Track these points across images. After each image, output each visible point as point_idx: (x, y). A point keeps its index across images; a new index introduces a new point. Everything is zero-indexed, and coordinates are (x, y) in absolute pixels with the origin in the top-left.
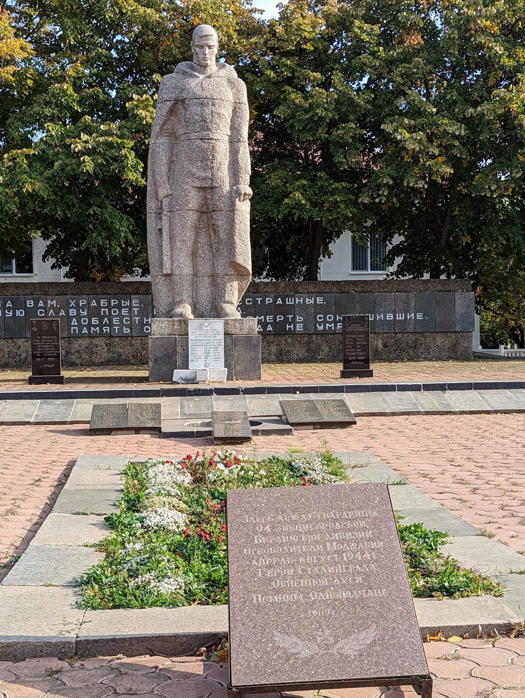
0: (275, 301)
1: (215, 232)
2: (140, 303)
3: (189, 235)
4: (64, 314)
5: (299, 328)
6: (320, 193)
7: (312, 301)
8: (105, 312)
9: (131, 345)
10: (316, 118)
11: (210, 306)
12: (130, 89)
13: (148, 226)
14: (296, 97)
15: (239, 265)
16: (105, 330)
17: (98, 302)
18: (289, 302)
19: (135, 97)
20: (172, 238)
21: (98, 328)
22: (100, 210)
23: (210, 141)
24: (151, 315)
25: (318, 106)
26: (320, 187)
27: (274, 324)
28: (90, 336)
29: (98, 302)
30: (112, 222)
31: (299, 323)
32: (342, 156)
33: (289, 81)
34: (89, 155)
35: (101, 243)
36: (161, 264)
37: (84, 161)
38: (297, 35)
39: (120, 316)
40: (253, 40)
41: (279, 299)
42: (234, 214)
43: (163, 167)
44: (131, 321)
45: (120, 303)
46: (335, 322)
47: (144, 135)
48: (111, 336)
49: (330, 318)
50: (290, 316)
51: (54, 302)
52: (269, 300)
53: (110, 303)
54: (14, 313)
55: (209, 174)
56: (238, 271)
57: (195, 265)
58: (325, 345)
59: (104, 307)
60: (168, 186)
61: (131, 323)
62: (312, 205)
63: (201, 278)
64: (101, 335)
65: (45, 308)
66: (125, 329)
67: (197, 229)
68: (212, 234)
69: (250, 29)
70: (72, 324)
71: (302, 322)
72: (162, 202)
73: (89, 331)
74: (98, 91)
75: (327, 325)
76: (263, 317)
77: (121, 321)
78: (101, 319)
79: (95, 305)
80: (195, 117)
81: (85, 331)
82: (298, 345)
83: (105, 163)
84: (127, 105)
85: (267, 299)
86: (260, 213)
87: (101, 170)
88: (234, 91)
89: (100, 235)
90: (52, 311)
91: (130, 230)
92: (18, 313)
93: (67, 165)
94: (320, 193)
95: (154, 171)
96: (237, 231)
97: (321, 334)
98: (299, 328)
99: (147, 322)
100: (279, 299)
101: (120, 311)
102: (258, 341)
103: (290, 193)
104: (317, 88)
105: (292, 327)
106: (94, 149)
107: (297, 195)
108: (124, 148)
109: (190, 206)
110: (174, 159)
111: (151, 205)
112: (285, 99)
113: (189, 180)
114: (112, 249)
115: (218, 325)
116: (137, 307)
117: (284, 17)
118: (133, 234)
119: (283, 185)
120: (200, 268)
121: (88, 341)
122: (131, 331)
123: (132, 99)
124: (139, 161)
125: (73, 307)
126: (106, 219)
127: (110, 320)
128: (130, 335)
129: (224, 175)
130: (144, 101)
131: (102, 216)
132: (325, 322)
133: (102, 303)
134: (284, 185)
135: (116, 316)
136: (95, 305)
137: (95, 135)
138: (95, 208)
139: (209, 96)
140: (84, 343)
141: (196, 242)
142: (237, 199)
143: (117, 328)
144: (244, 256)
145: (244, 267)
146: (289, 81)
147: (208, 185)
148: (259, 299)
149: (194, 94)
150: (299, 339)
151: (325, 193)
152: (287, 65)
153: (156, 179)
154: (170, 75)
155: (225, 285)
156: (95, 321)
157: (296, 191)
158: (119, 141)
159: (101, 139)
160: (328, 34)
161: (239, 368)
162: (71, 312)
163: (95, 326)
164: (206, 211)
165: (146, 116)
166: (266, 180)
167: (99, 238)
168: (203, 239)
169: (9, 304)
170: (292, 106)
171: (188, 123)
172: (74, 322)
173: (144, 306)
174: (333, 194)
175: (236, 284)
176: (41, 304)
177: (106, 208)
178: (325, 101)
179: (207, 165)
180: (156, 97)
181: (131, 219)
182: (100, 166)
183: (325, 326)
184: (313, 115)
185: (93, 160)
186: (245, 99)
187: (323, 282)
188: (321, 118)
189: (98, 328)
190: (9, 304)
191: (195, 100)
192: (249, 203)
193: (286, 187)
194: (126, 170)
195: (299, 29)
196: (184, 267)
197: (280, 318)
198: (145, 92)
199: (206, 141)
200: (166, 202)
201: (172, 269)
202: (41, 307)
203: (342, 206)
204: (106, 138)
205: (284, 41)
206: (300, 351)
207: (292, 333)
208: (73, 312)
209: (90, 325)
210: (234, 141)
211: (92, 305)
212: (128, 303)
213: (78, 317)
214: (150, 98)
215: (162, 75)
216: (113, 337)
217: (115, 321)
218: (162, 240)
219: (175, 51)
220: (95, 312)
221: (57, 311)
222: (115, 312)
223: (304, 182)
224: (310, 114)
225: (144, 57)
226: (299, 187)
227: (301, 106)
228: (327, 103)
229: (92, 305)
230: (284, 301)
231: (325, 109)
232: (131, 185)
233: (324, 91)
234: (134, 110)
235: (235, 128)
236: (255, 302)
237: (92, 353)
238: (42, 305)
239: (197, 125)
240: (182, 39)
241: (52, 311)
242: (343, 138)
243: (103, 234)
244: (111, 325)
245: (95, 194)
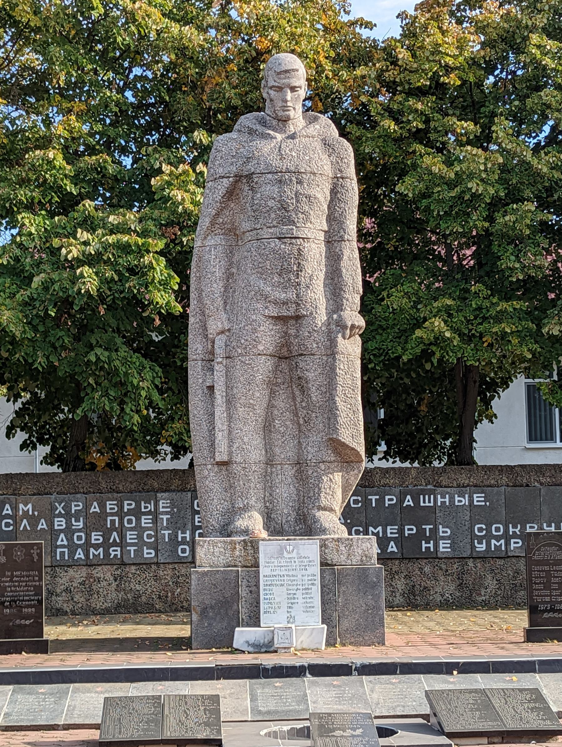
0: (401, 500)
1: (303, 390)
2: (172, 506)
3: (259, 396)
4: (45, 526)
5: (444, 547)
6: (475, 318)
8: (113, 522)
9: (157, 578)
10: (467, 197)
11: (294, 515)
12: (157, 156)
13: (190, 382)
14: (434, 163)
15: (344, 445)
16: (113, 554)
17: (102, 506)
18: (426, 502)
19: (166, 168)
20: (230, 402)
21: (101, 550)
22: (106, 354)
23: (294, 241)
24: (189, 526)
25: (471, 176)
26: (476, 309)
27: (401, 540)
28: (89, 564)
29: (102, 506)
30: (126, 374)
31: (443, 538)
32: (513, 258)
33: (420, 136)
34: (90, 265)
35: (107, 408)
36: (212, 445)
37: (82, 276)
38: (434, 61)
39: (139, 528)
40: (360, 71)
41: (409, 497)
42: (334, 359)
43: (215, 285)
44: (156, 536)
45: (138, 506)
46: (507, 537)
47: (180, 230)
48: (123, 564)
49: (498, 529)
50: (428, 527)
51: (30, 506)
52: (390, 500)
53: (121, 507)
55: (291, 295)
56: (343, 455)
57: (268, 447)
58: (489, 577)
59: (112, 514)
60: (224, 316)
61: (157, 540)
62: (462, 340)
63: (279, 467)
64: (107, 561)
65: (13, 517)
66: (146, 551)
67: (272, 387)
68: (297, 393)
69: (352, 54)
70: (59, 543)
71: (448, 538)
72: (213, 342)
73: (87, 555)
74: (105, 161)
75: (493, 542)
76: (380, 528)
77: (140, 537)
78: (106, 535)
79: (97, 510)
80: (269, 203)
81: (80, 554)
82: (442, 578)
83: (116, 278)
84: (153, 181)
85: (387, 497)
86: (374, 355)
87: (110, 289)
88: (333, 158)
89: (107, 395)
90: (25, 521)
91: (157, 386)
93: (53, 282)
94: (475, 318)
95: (200, 291)
96: (339, 388)
97: (482, 558)
98: (444, 547)
99: (184, 538)
100: (409, 497)
101: (138, 520)
102: (378, 577)
103: (425, 320)
104: (469, 148)
105: (431, 545)
106: (99, 254)
107: (436, 324)
108: (148, 252)
109: (261, 348)
110: (234, 270)
111: (195, 347)
112: (415, 166)
113: (259, 306)
114: (127, 418)
115: (309, 549)
116: (166, 513)
117: (410, 32)
118: (161, 392)
119: (412, 307)
120: (277, 450)
121: (84, 572)
122: (157, 555)
123: (160, 171)
124: (172, 273)
125: (60, 515)
126: (117, 370)
127: (122, 536)
128: (155, 560)
129: (317, 296)
130: (180, 175)
131: (109, 364)
132: (489, 537)
133: (108, 507)
134: (415, 307)
135: (131, 529)
136: (97, 510)
137: (100, 231)
138: (99, 351)
139: (293, 169)
140: (78, 575)
141: (270, 406)
142: (340, 335)
143: (132, 549)
144: (352, 428)
145: (353, 449)
146: (420, 136)
147: (291, 313)
148: (374, 498)
149: (268, 165)
150: (444, 567)
151: (485, 318)
152: (416, 110)
153: (204, 305)
154: (227, 135)
155: (319, 479)
156: (96, 537)
157: (435, 316)
158: (140, 241)
159: (111, 239)
160: (484, 57)
161: (345, 624)
162: (56, 523)
163: (96, 547)
164: (287, 356)
165: (183, 199)
166: (383, 299)
167: (105, 400)
168: (281, 402)
170: (426, 177)
171: (257, 213)
172: (62, 540)
173: (179, 511)
174: (498, 319)
175: (338, 477)
177: (117, 350)
178: (482, 168)
179: (290, 280)
180: (201, 167)
181: (157, 368)
182: (108, 283)
183: (488, 544)
184: (463, 192)
185: (97, 274)
186: (351, 171)
187: (484, 467)
188: (476, 196)
189: (101, 550)
191: (270, 176)
192: (358, 340)
193: (418, 310)
194: (150, 288)
195: (436, 51)
196: (250, 448)
197: (410, 530)
198: (182, 161)
199: (288, 241)
200: (220, 342)
201: (230, 453)
202: (7, 516)
203: (515, 341)
204: (119, 236)
205: (411, 72)
206: (447, 587)
207: (433, 557)
208: (60, 523)
209: (88, 545)
210: (333, 240)
211: (92, 510)
212: (151, 507)
213: (69, 531)
214: (191, 171)
215: (210, 131)
216: (125, 565)
217: (130, 537)
218: (213, 405)
219: (230, 93)
220: (96, 522)
221: (33, 521)
222: (129, 522)
223: (449, 302)
224: (458, 189)
225: (179, 103)
226: (440, 311)
227: (442, 177)
228: (486, 170)
229: (92, 510)
230: (416, 500)
231: (482, 180)
232: (160, 313)
233: (480, 151)
234: (163, 189)
235: (335, 219)
237: (90, 592)
238: (10, 512)
239: (273, 216)
240: (242, 73)
241: (25, 521)
242: (514, 229)
243: (112, 393)
244: (122, 544)
245: (98, 327)
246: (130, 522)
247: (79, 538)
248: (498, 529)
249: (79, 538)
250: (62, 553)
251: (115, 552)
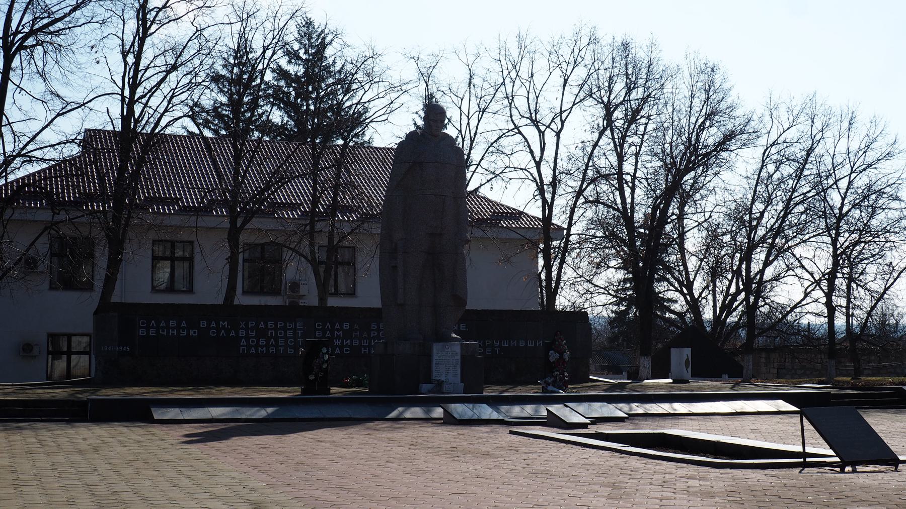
17: (266, 325)
29: (266, 325)
73: (257, 350)
101: (285, 332)
125: (242, 328)
127: (276, 341)
156: (262, 341)
163: (262, 347)
169: (184, 324)
172: (243, 342)
176: (213, 325)
190: (184, 324)
208: (242, 333)
209: (257, 346)
213: (247, 338)
217: (281, 342)
246: (281, 333)
247: (253, 342)
249: (253, 342)
250: (243, 350)
251: (272, 350)
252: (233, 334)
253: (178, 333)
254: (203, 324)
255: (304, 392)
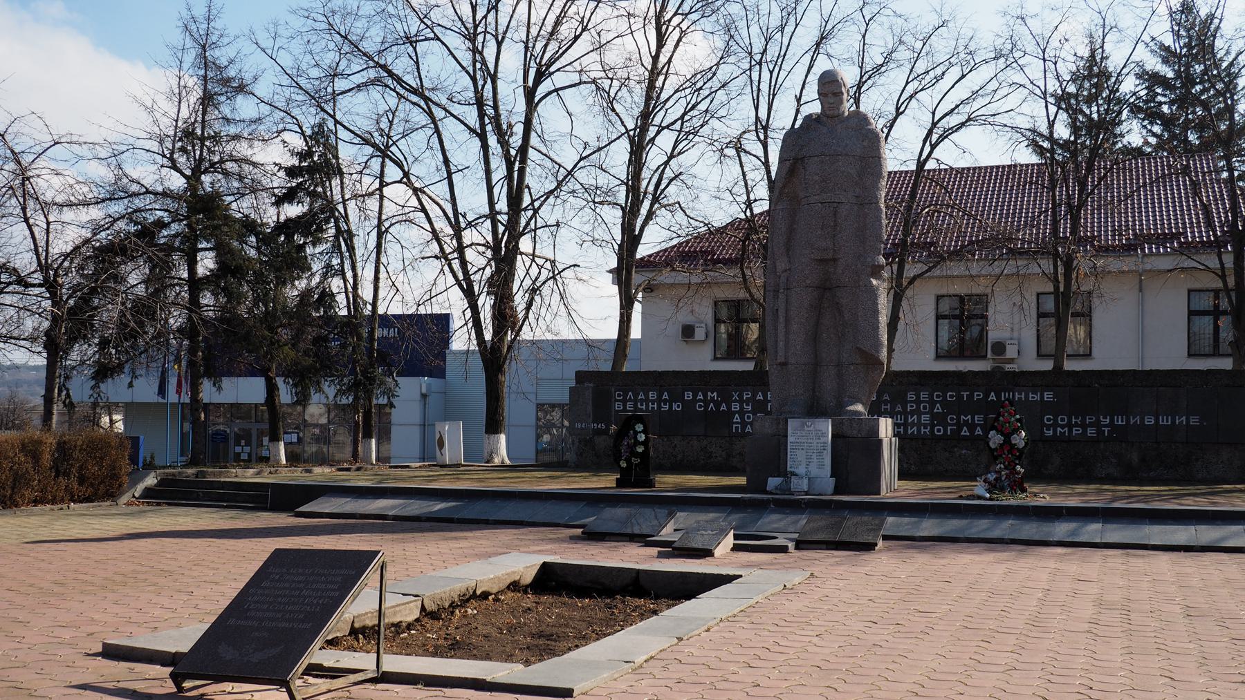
7: (1037, 397)
54: (671, 406)
92: (675, 407)
125: (735, 401)
132: (1055, 425)
169: (665, 396)
172: (737, 418)
176: (700, 396)
183: (1055, 431)
190: (665, 396)
202: (700, 400)
208: (735, 407)
213: (742, 412)
220: (760, 407)
221: (718, 405)
230: (998, 396)
236: (960, 397)
248: (1063, 420)
252: (723, 408)
253: (659, 407)
254: (688, 396)
255: (620, 483)
